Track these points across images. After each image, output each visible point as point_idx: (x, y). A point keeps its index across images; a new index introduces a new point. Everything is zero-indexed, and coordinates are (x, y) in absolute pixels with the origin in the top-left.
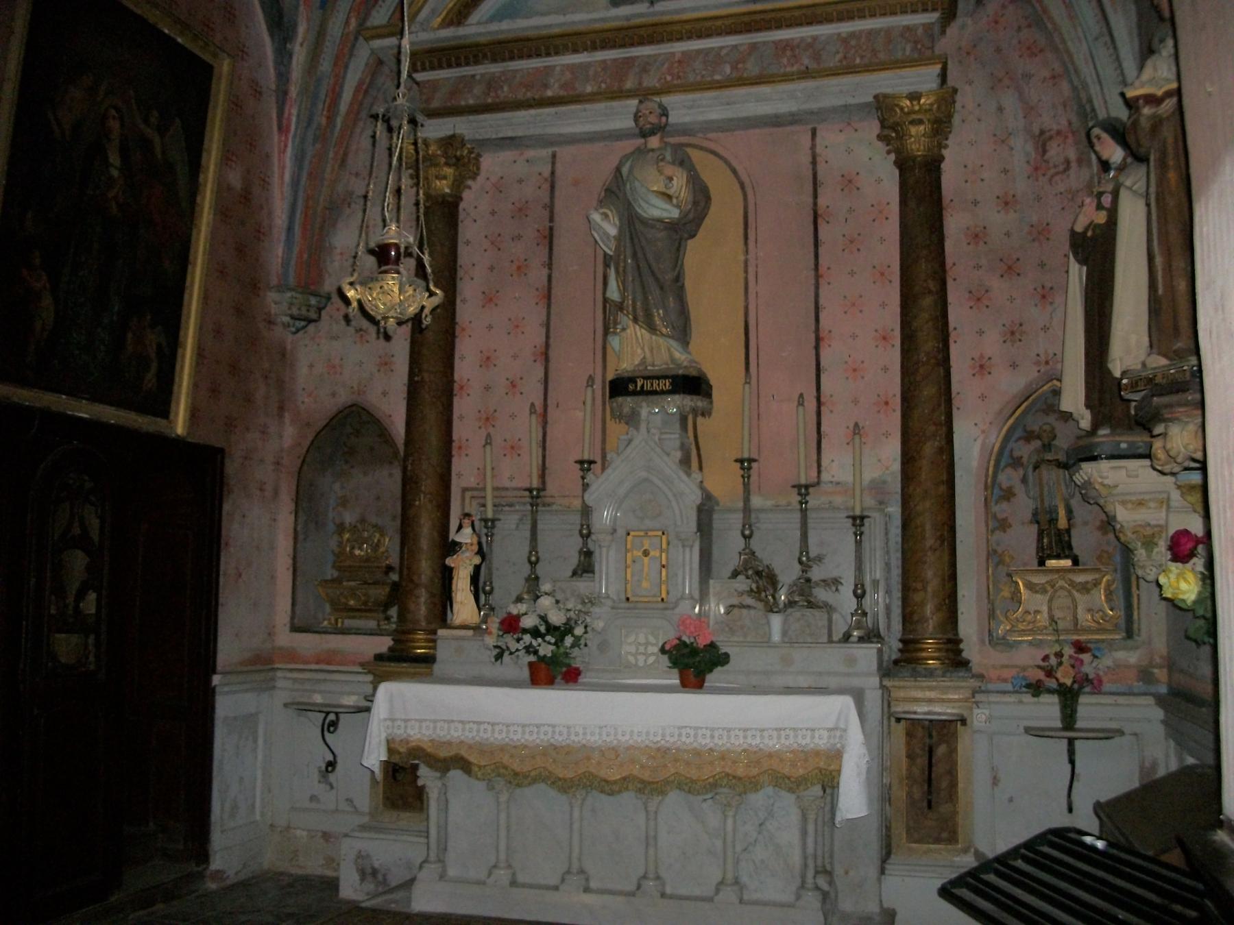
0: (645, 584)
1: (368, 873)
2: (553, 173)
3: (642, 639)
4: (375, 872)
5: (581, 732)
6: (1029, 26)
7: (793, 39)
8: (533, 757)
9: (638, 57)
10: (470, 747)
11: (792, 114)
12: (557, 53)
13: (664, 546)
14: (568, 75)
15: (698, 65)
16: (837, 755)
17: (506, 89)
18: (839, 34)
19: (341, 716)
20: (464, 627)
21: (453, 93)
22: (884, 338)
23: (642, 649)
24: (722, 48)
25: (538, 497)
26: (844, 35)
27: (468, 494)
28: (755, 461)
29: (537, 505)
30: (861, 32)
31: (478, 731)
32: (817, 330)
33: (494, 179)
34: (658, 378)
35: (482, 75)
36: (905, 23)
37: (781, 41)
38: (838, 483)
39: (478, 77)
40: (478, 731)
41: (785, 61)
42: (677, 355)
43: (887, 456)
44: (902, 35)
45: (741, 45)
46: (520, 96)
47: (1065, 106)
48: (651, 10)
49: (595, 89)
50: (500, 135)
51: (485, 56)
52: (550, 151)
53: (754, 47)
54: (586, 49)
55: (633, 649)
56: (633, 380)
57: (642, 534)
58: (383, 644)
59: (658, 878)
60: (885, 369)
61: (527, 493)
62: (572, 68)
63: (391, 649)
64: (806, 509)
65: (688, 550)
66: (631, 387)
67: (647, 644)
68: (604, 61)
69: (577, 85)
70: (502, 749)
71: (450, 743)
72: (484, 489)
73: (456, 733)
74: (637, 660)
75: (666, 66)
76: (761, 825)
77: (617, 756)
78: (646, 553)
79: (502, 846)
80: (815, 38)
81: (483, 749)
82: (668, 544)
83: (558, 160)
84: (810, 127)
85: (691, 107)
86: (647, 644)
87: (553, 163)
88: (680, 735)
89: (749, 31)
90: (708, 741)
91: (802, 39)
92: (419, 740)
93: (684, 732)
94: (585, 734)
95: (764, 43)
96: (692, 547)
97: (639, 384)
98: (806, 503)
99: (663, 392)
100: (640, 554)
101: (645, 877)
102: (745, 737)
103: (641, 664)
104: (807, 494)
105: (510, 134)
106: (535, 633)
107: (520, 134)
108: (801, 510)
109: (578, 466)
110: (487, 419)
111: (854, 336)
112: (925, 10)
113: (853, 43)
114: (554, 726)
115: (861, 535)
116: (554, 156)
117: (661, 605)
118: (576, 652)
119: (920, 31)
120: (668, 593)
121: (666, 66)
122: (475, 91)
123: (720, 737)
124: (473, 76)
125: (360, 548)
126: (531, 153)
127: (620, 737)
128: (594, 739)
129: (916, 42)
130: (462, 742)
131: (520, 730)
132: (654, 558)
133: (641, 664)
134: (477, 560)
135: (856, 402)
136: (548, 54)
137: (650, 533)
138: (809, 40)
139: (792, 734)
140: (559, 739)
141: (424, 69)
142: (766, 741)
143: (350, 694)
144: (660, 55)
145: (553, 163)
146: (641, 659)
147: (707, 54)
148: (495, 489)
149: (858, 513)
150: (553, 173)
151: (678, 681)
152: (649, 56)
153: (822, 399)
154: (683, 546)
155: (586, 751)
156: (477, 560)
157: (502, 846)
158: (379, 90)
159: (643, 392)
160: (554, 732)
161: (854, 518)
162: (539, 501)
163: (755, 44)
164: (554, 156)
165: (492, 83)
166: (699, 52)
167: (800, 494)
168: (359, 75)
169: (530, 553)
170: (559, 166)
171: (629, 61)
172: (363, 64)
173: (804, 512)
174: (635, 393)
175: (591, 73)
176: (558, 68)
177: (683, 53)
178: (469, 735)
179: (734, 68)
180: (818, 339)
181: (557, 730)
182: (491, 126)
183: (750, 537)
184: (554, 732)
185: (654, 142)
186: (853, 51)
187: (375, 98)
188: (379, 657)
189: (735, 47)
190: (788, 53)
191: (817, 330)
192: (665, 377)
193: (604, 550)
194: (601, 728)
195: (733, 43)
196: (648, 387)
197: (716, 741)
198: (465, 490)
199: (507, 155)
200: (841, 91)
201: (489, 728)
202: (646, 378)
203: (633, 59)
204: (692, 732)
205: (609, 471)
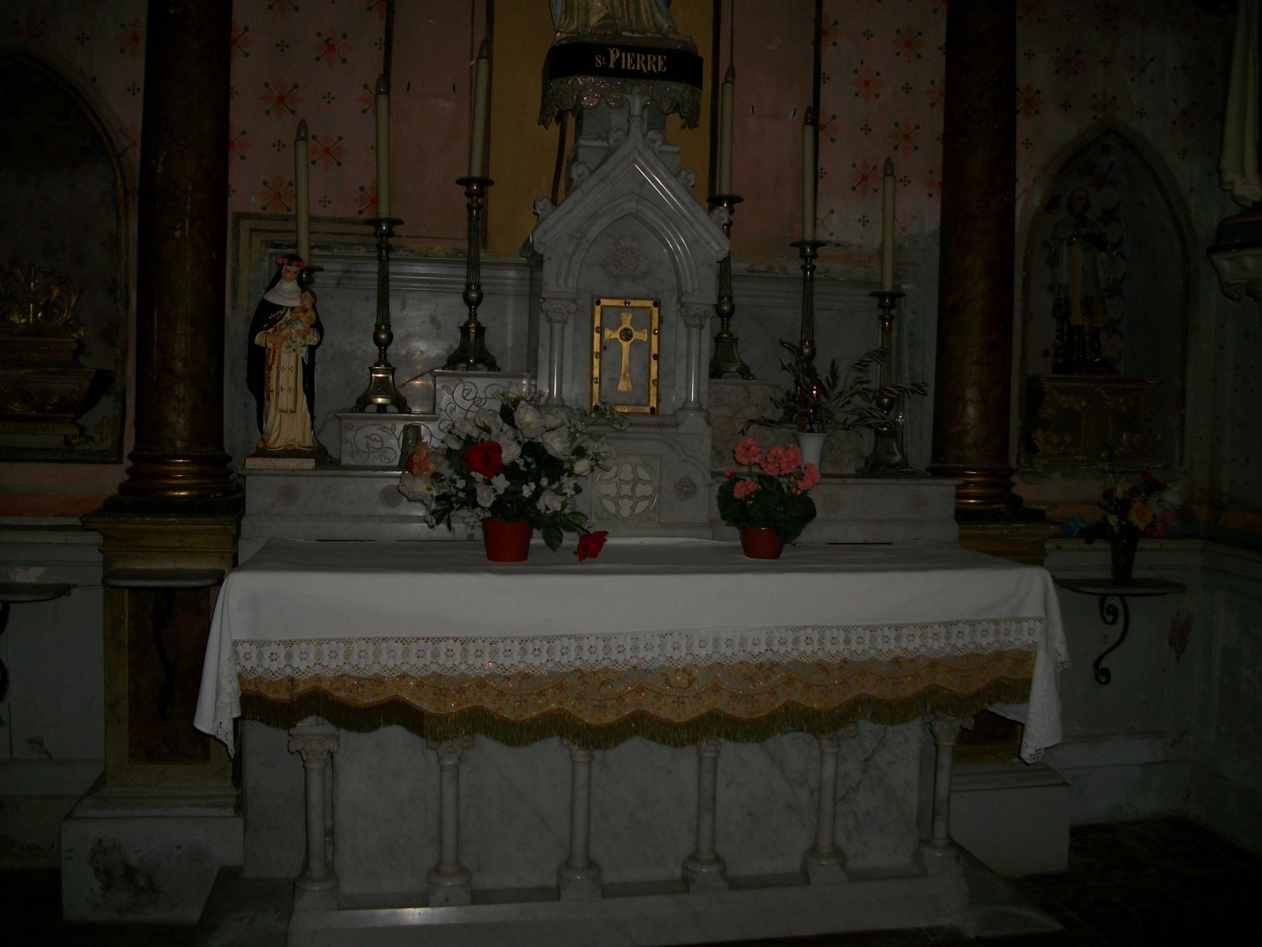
0: (623, 385)
1: (118, 873)
3: (627, 474)
4: (130, 873)
5: (628, 646)
8: (542, 694)
10: (420, 684)
13: (655, 324)
16: (1025, 659)
19: (12, 606)
20: (291, 453)
22: (909, 44)
23: (626, 489)
25: (390, 234)
27: (245, 225)
28: (740, 200)
29: (389, 248)
31: (435, 655)
32: (818, 20)
34: (645, 50)
38: (838, 245)
40: (435, 655)
42: (660, 18)
43: (921, 211)
55: (611, 489)
56: (603, 50)
57: (620, 303)
58: (111, 478)
59: (718, 859)
60: (907, 88)
61: (372, 229)
63: (122, 488)
64: (812, 278)
65: (695, 331)
66: (599, 62)
67: (636, 481)
70: (481, 683)
71: (378, 680)
72: (295, 218)
73: (391, 661)
74: (618, 507)
76: (866, 760)
77: (690, 683)
78: (627, 335)
79: (449, 840)
81: (439, 684)
82: (660, 321)
86: (636, 481)
88: (796, 641)
90: (841, 647)
92: (318, 678)
93: (802, 635)
94: (635, 648)
96: (701, 327)
97: (613, 58)
98: (813, 268)
99: (651, 76)
100: (616, 335)
101: (695, 857)
102: (898, 639)
103: (625, 512)
104: (815, 256)
106: (511, 472)
108: (805, 279)
109: (463, 189)
110: (281, 100)
111: (869, 35)
114: (579, 638)
115: (891, 319)
117: (652, 419)
118: (578, 498)
120: (658, 401)
123: (860, 640)
125: (25, 314)
127: (696, 650)
128: (651, 656)
130: (404, 676)
131: (516, 647)
132: (638, 343)
133: (625, 512)
134: (313, 339)
135: (866, 129)
137: (634, 303)
139: (967, 629)
140: (592, 659)
142: (930, 643)
143: (28, 564)
146: (626, 505)
148: (313, 219)
149: (888, 287)
151: (739, 543)
153: (821, 122)
154: (687, 325)
155: (639, 677)
156: (313, 339)
157: (449, 840)
159: (618, 72)
160: (580, 648)
161: (881, 296)
162: (391, 241)
167: (803, 256)
169: (378, 326)
173: (808, 283)
174: (605, 72)
178: (417, 662)
180: (819, 33)
181: (586, 644)
183: (730, 314)
184: (580, 648)
188: (113, 506)
191: (818, 20)
192: (657, 51)
193: (557, 326)
194: (663, 636)
196: (627, 62)
197: (854, 646)
198: (239, 217)
201: (458, 648)
202: (624, 48)
204: (815, 635)
205: (575, 196)
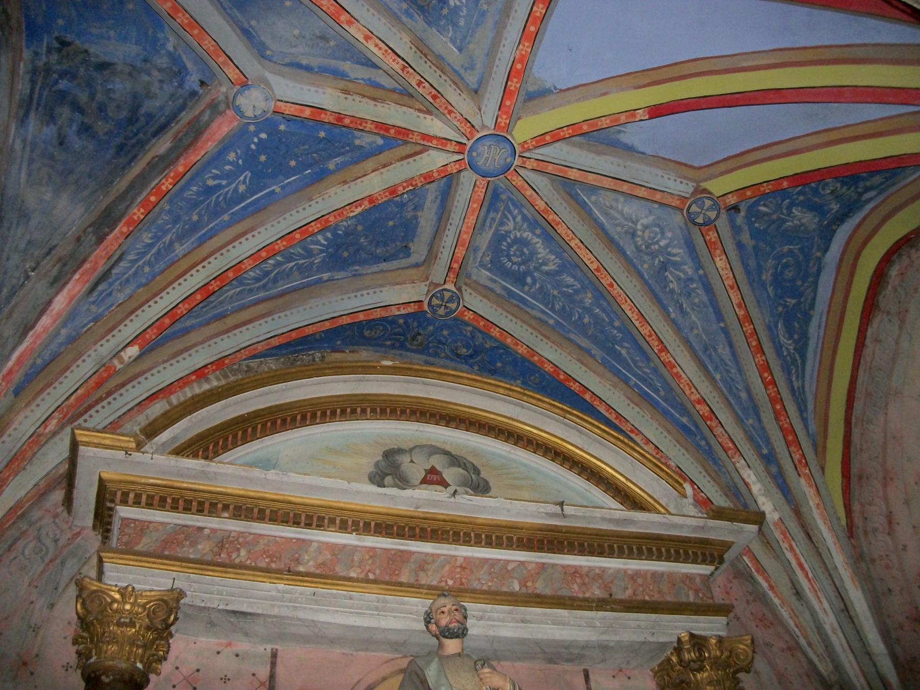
2: (272, 676)
6: (754, 600)
7: (581, 567)
9: (414, 553)
11: (586, 646)
12: (320, 526)
14: (327, 556)
15: (482, 574)
17: (243, 553)
18: (625, 571)
21: (166, 543)
24: (509, 561)
26: (630, 572)
30: (646, 572)
33: (185, 671)
35: (214, 531)
36: (685, 571)
37: (569, 566)
39: (206, 532)
41: (575, 587)
44: (683, 582)
45: (529, 562)
46: (263, 564)
47: (808, 676)
48: (452, 499)
49: (362, 576)
50: (230, 608)
51: (226, 507)
52: (269, 647)
53: (543, 567)
54: (357, 530)
62: (334, 549)
68: (373, 549)
69: (338, 569)
75: (447, 568)
80: (603, 570)
83: (279, 660)
84: (582, 668)
85: (481, 618)
87: (273, 664)
89: (540, 549)
91: (591, 569)
95: (554, 566)
105: (244, 608)
107: (259, 611)
112: (704, 562)
113: (640, 581)
116: (274, 655)
119: (698, 580)
121: (447, 568)
122: (200, 547)
124: (201, 529)
126: (243, 645)
129: (697, 591)
136: (308, 525)
138: (597, 571)
141: (137, 503)
144: (439, 555)
145: (273, 664)
147: (492, 566)
150: (272, 676)
152: (427, 554)
158: (31, 524)
163: (544, 564)
164: (274, 655)
165: (224, 542)
166: (486, 560)
168: (23, 493)
170: (280, 670)
171: (403, 556)
172: (33, 482)
175: (356, 558)
176: (315, 545)
177: (465, 558)
179: (523, 584)
182: (220, 593)
185: (452, 646)
186: (641, 589)
187: (24, 533)
189: (522, 563)
190: (578, 580)
195: (522, 559)
199: (208, 641)
200: (639, 627)
203: (411, 553)
